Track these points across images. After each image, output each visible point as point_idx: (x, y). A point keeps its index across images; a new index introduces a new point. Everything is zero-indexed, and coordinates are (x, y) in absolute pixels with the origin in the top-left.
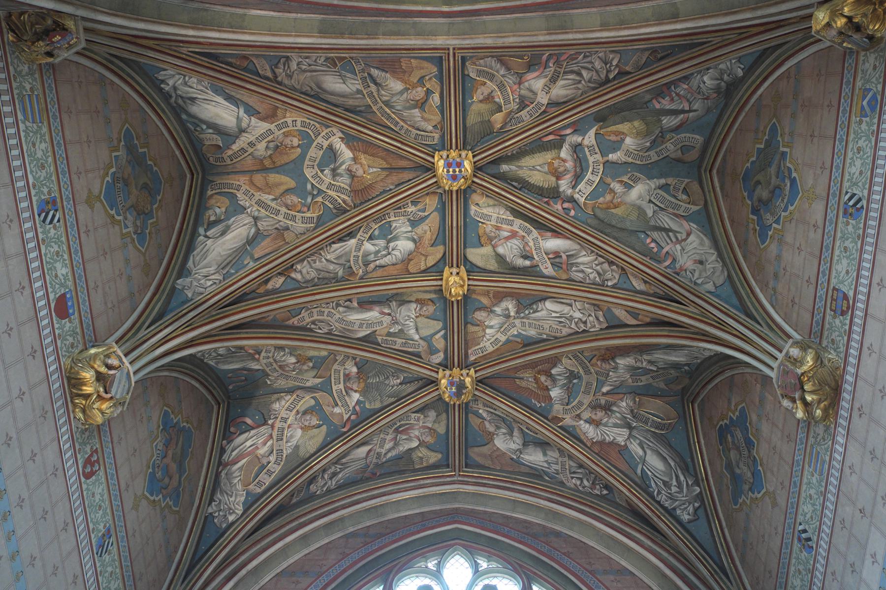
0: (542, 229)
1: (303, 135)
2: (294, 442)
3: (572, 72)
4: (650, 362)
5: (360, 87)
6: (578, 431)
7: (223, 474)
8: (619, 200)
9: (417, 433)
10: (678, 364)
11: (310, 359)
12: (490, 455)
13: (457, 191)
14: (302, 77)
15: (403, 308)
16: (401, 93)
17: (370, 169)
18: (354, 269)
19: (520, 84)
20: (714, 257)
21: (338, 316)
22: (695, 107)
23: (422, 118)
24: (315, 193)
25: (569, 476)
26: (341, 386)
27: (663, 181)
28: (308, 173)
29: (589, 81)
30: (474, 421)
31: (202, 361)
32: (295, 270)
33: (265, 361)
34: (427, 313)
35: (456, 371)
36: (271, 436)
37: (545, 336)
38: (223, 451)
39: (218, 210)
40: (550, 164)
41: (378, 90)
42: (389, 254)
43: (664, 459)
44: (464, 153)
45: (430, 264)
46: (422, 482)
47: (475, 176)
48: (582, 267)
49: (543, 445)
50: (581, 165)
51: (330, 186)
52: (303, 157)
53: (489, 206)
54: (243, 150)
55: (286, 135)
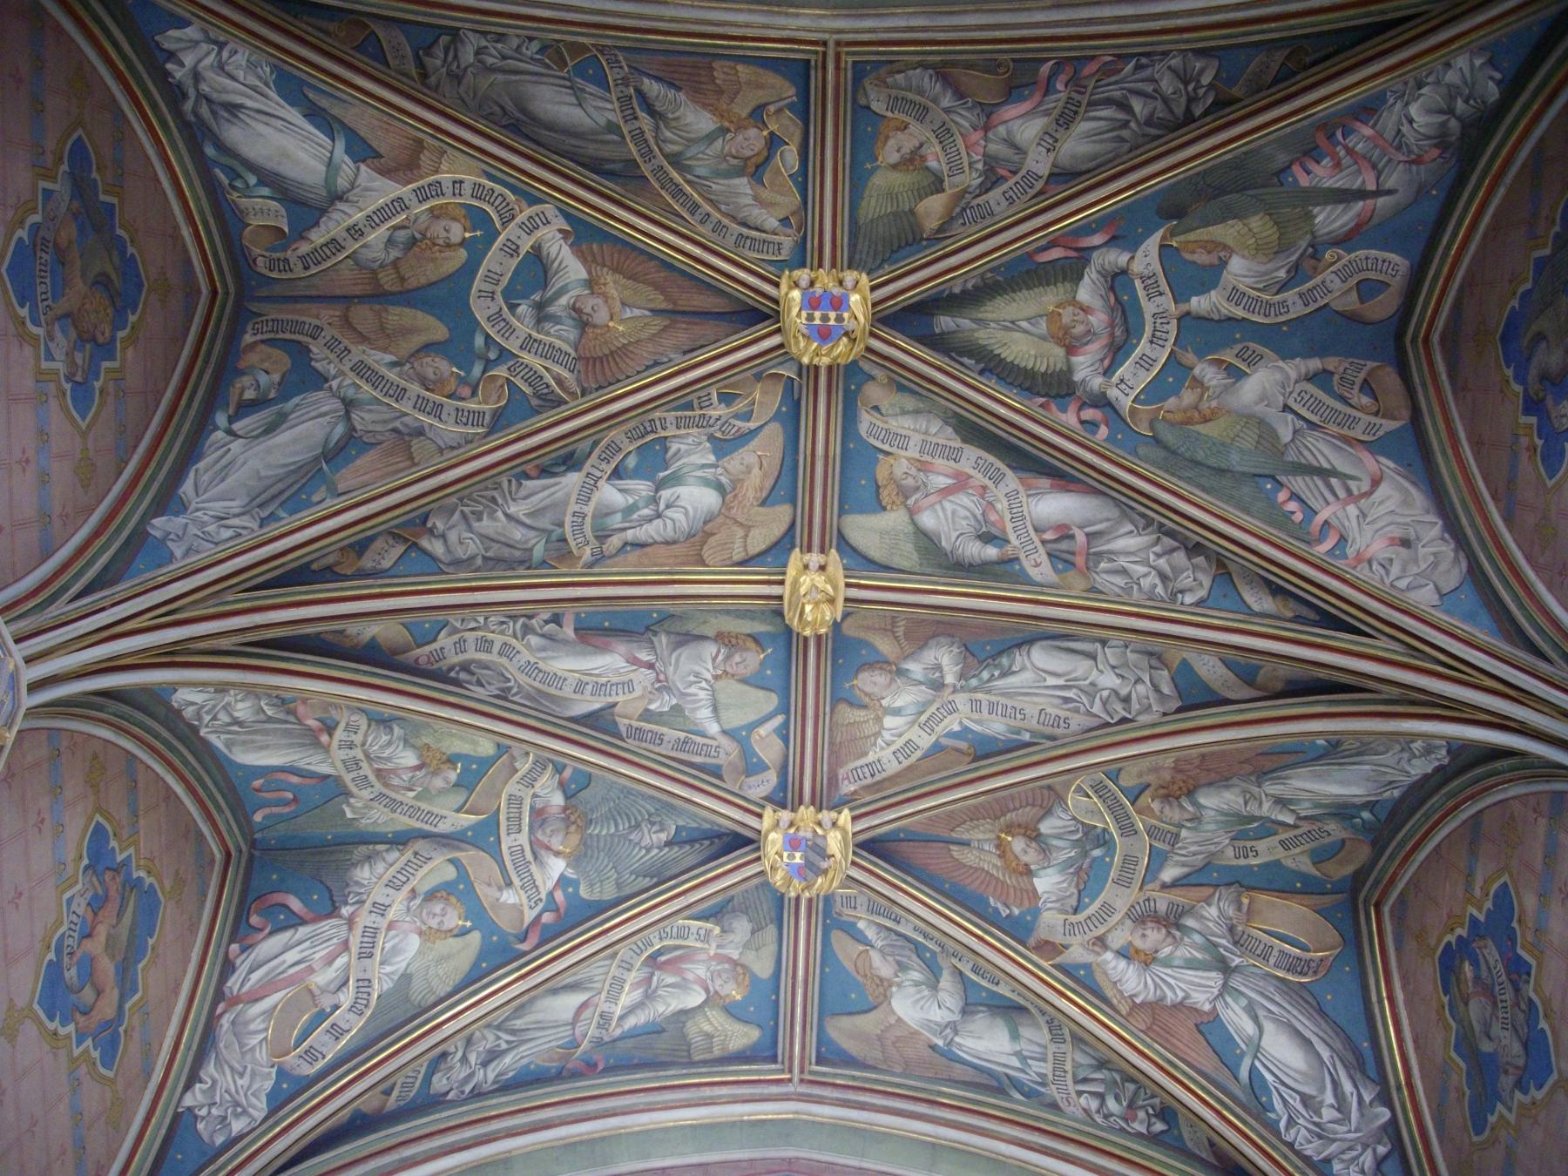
0: (1022, 469)
1: (477, 218)
2: (399, 965)
3: (1109, 102)
4: (1281, 802)
5: (616, 117)
6: (1099, 977)
7: (225, 1022)
8: (1214, 404)
9: (701, 971)
10: (1345, 806)
11: (451, 760)
12: (879, 1038)
13: (830, 368)
14: (484, 83)
15: (686, 652)
16: (710, 138)
17: (623, 313)
18: (572, 543)
19: (986, 129)
20: (1436, 531)
21: (526, 656)
23: (755, 198)
24: (492, 355)
25: (1072, 1088)
26: (523, 839)
27: (1315, 364)
28: (481, 310)
29: (1149, 122)
30: (845, 949)
31: (195, 730)
32: (431, 531)
33: (343, 754)
34: (741, 670)
35: (806, 813)
36: (345, 946)
37: (1026, 737)
38: (228, 967)
39: (263, 379)
40: (1053, 317)
41: (657, 128)
42: (659, 516)
43: (1307, 1043)
44: (850, 277)
45: (753, 550)
46: (707, 1092)
47: (872, 334)
48: (1122, 562)
49: (1011, 1011)
50: (1126, 321)
51: (528, 344)
52: (469, 269)
53: (904, 412)
54: (334, 245)
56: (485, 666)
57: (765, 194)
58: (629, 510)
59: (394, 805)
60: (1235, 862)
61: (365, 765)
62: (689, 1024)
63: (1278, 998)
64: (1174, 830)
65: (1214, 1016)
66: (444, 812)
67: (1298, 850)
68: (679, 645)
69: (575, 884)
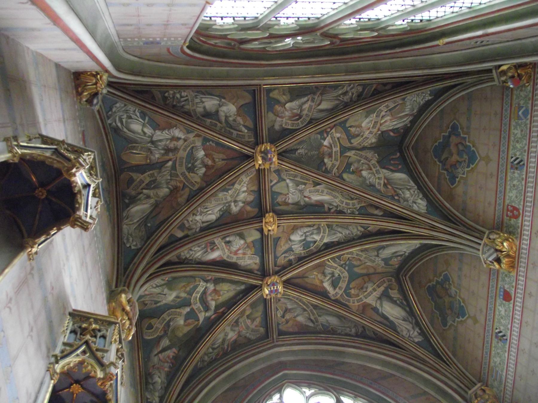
1: (349, 295)
2: (368, 120)
3: (217, 348)
4: (148, 197)
7: (415, 111)
11: (353, 172)
15: (296, 200)
16: (297, 316)
19: (239, 332)
21: (337, 200)
22: (156, 357)
24: (344, 266)
26: (334, 150)
27: (158, 305)
28: (346, 274)
33: (381, 175)
34: (282, 196)
36: (381, 125)
42: (305, 233)
48: (199, 249)
51: (336, 268)
55: (358, 295)
56: (347, 199)
57: (284, 305)
58: (312, 234)
59: (366, 158)
60: (154, 171)
61: (375, 172)
62: (289, 98)
63: (138, 139)
64: (173, 178)
65: (155, 130)
66: (353, 156)
67: (138, 180)
68: (299, 202)
69: (321, 139)
